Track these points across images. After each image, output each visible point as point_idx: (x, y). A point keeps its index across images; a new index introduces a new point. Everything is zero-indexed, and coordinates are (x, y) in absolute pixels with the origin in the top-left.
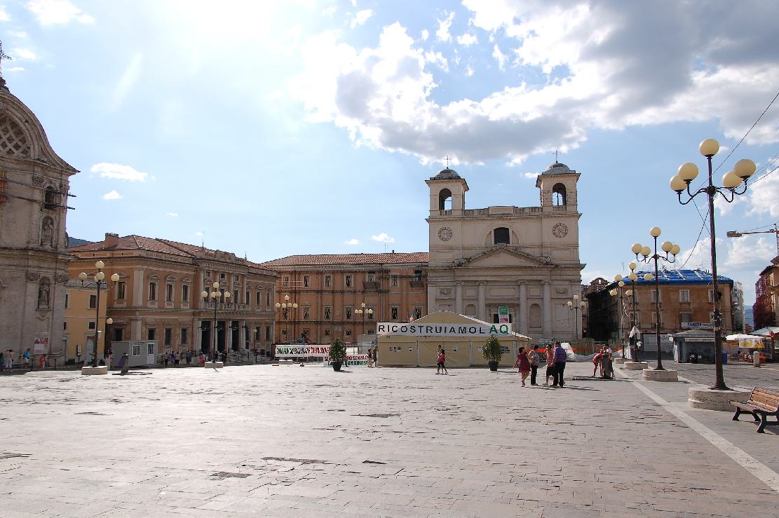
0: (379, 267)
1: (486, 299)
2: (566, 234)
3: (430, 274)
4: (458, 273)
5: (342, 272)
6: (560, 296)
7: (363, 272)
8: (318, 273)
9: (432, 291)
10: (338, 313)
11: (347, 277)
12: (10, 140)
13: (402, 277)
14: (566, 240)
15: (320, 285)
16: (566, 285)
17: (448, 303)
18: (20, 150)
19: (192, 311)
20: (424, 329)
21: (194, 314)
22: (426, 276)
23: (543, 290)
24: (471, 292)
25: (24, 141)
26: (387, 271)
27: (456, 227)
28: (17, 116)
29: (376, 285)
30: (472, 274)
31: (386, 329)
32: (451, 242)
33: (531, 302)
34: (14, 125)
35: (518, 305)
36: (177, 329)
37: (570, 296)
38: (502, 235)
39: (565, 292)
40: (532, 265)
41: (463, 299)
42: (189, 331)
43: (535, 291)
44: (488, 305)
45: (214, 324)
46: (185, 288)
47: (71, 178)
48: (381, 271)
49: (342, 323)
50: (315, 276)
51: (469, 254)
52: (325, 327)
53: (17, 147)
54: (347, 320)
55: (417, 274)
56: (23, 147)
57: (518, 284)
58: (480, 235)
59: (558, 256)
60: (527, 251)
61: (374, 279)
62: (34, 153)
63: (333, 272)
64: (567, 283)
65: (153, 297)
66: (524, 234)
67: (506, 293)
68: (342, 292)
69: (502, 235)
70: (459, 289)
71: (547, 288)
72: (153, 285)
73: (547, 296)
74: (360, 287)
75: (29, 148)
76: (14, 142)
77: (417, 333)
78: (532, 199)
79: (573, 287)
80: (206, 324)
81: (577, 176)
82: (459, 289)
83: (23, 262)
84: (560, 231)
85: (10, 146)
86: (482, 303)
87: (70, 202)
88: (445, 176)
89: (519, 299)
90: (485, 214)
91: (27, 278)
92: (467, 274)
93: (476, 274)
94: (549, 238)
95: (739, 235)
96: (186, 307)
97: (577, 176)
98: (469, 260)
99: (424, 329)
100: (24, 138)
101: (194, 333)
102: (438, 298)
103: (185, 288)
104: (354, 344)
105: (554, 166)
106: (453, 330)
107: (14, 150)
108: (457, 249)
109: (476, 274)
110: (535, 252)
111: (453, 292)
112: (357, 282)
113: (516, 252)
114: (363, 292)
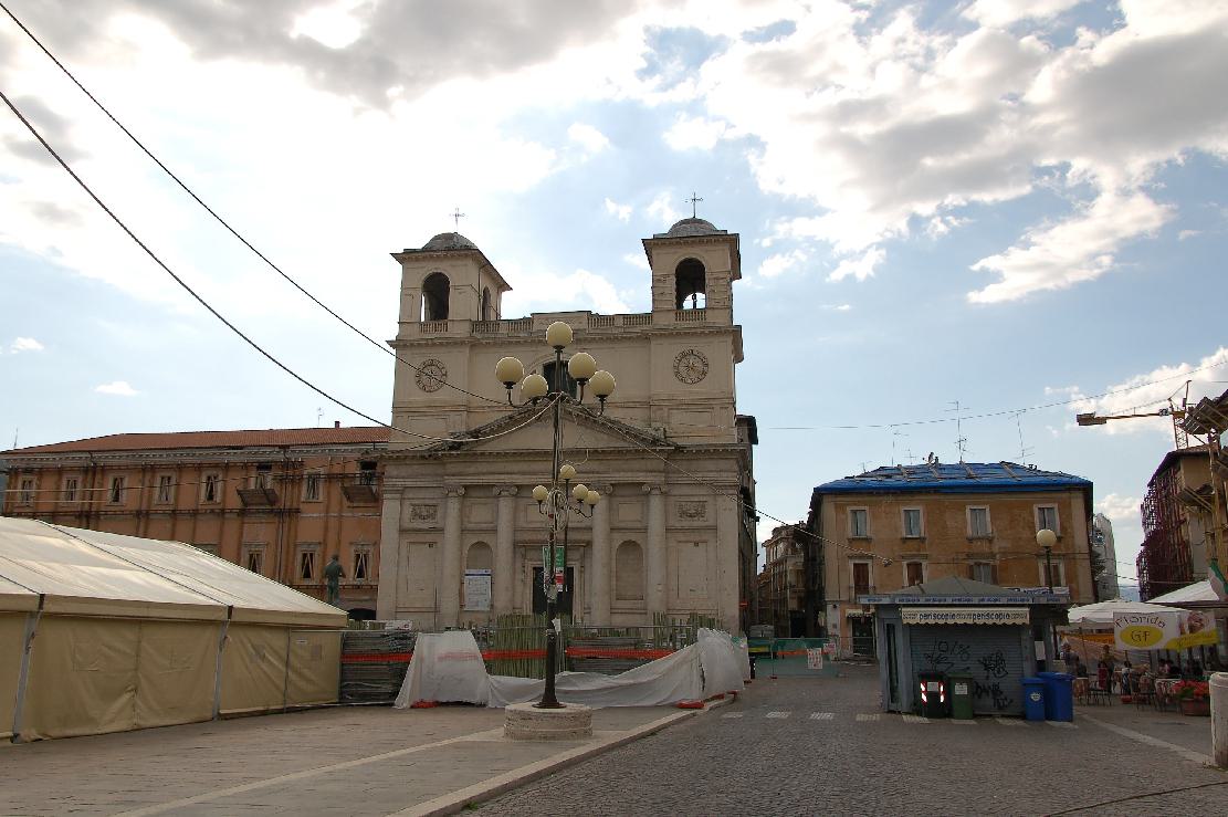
2: (704, 373)
3: (391, 470)
6: (686, 523)
9: (390, 507)
11: (209, 478)
13: (330, 478)
15: (145, 500)
30: (483, 467)
32: (443, 395)
33: (619, 539)
35: (589, 544)
37: (711, 522)
39: (699, 514)
40: (620, 444)
44: (516, 545)
48: (286, 465)
51: (478, 422)
59: (689, 428)
63: (180, 468)
64: (703, 491)
68: (195, 513)
70: (453, 506)
71: (656, 503)
73: (656, 523)
74: (234, 502)
79: (720, 499)
84: (690, 368)
86: (503, 543)
92: (472, 469)
93: (493, 468)
94: (665, 385)
95: (1102, 421)
102: (407, 525)
109: (493, 468)
110: (635, 419)
112: (228, 493)
114: (242, 513)
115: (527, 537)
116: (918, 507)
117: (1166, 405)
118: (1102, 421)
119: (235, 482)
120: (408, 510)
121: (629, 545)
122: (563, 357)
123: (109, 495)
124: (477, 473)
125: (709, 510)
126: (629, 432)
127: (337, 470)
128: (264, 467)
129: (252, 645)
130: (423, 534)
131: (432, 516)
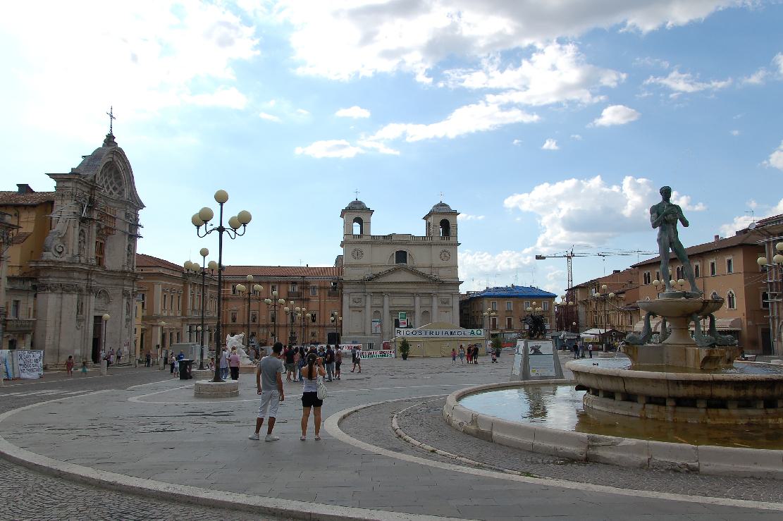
1: (390, 307)
3: (345, 286)
4: (368, 286)
6: (444, 305)
9: (345, 298)
10: (263, 317)
12: (111, 183)
13: (320, 288)
14: (449, 263)
16: (449, 296)
17: (360, 309)
18: (117, 192)
20: (428, 333)
22: (341, 288)
23: (432, 300)
24: (377, 301)
25: (120, 184)
26: (307, 283)
27: (366, 249)
28: (120, 165)
29: (299, 294)
31: (402, 333)
33: (423, 310)
34: (117, 172)
35: (414, 312)
37: (451, 305)
38: (401, 256)
39: (447, 302)
40: (425, 280)
41: (372, 307)
43: (426, 301)
47: (140, 212)
48: (302, 283)
49: (268, 326)
51: (377, 271)
52: (251, 330)
53: (115, 189)
54: (313, 324)
55: (331, 284)
56: (119, 189)
57: (413, 295)
58: (384, 257)
59: (443, 275)
60: (420, 270)
61: (297, 289)
62: (126, 195)
64: (448, 295)
66: (419, 258)
67: (406, 302)
69: (401, 256)
70: (368, 298)
71: (435, 299)
75: (124, 190)
76: (114, 185)
77: (423, 335)
78: (420, 230)
81: (455, 214)
82: (368, 298)
83: (120, 282)
85: (111, 189)
87: (140, 231)
88: (358, 207)
89: (414, 307)
90: (388, 239)
91: (123, 294)
94: (437, 261)
95: (544, 258)
97: (455, 214)
98: (377, 276)
99: (428, 333)
100: (121, 182)
104: (492, 344)
105: (436, 206)
106: (446, 333)
107: (113, 191)
108: (366, 265)
110: (427, 271)
111: (363, 300)
113: (413, 271)
115: (393, 309)
116: (511, 301)
117: (565, 254)
118: (544, 258)
119: (283, 287)
120: (351, 300)
121: (426, 313)
122: (400, 248)
123: (231, 293)
124: (377, 288)
125: (451, 301)
126: (422, 275)
127: (322, 285)
128: (294, 283)
129: (202, 344)
130: (358, 309)
131: (360, 302)
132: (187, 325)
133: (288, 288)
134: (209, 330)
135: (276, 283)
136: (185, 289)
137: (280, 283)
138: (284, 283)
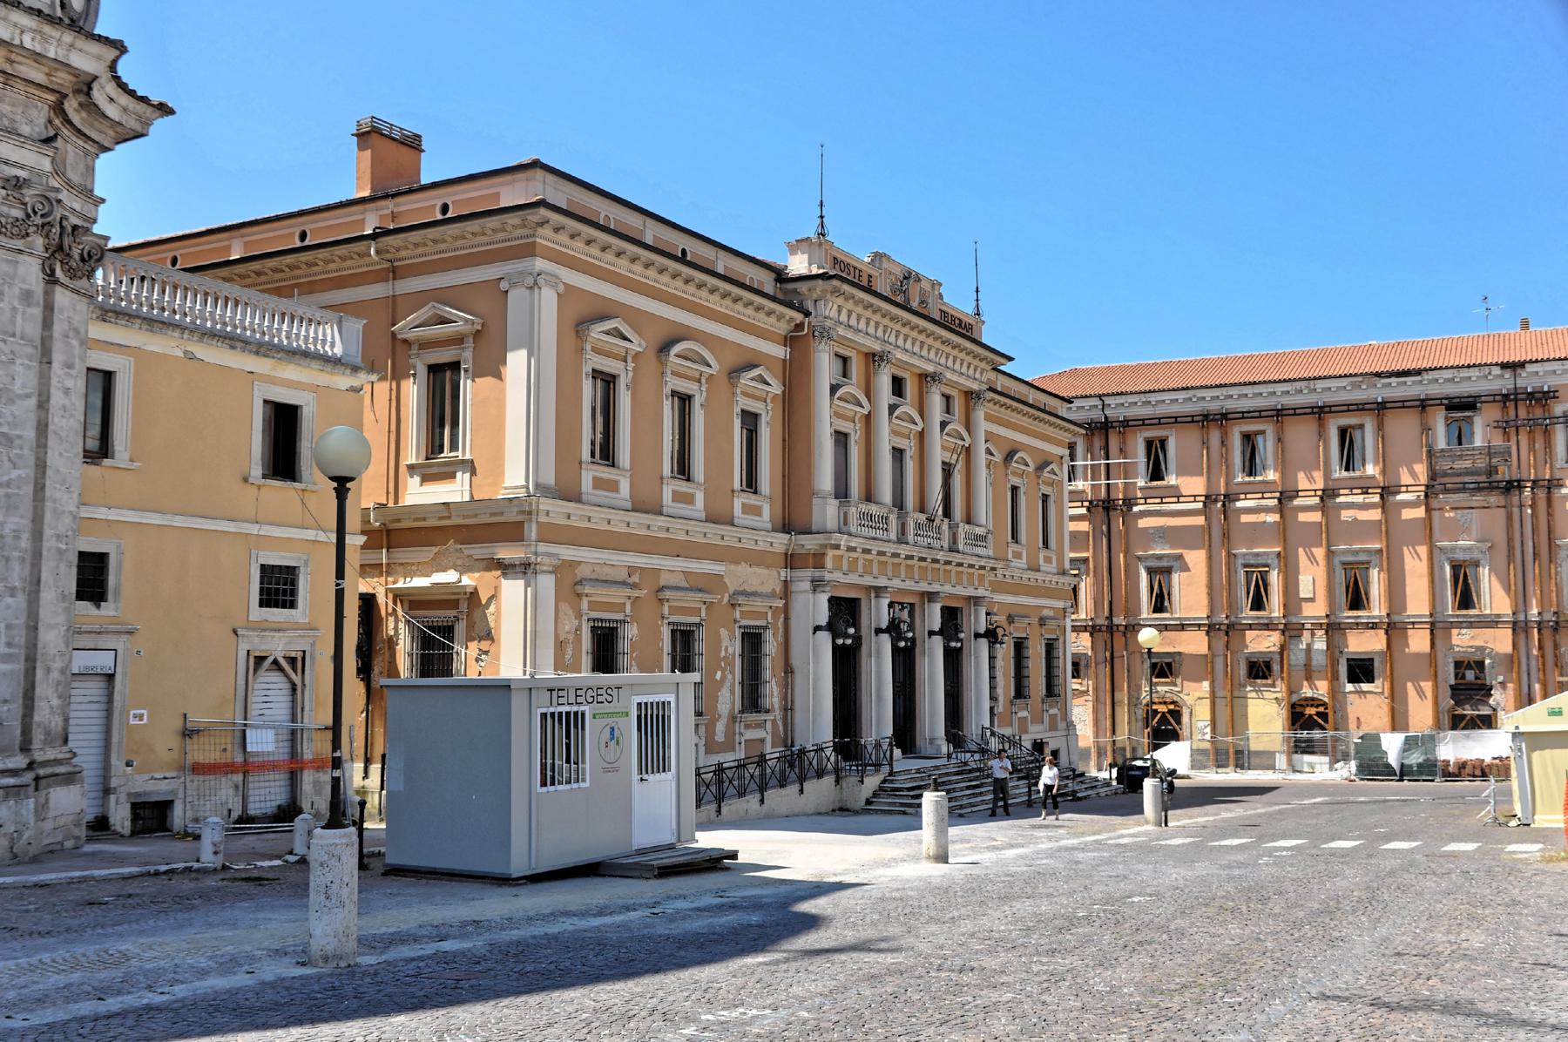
0: (1505, 383)
5: (1320, 412)
7: (1423, 405)
8: (1206, 420)
11: (1343, 432)
19: (780, 541)
21: (791, 560)
26: (1543, 398)
36: (724, 633)
42: (771, 646)
45: (878, 613)
46: (750, 421)
50: (1192, 436)
65: (606, 452)
72: (607, 381)
80: (845, 611)
96: (756, 519)
101: (795, 661)
103: (750, 421)
128: (1462, 406)
132: (817, 585)
133: (1426, 429)
134: (991, 635)
135: (1360, 407)
136: (795, 376)
137: (1381, 408)
138: (1403, 404)
